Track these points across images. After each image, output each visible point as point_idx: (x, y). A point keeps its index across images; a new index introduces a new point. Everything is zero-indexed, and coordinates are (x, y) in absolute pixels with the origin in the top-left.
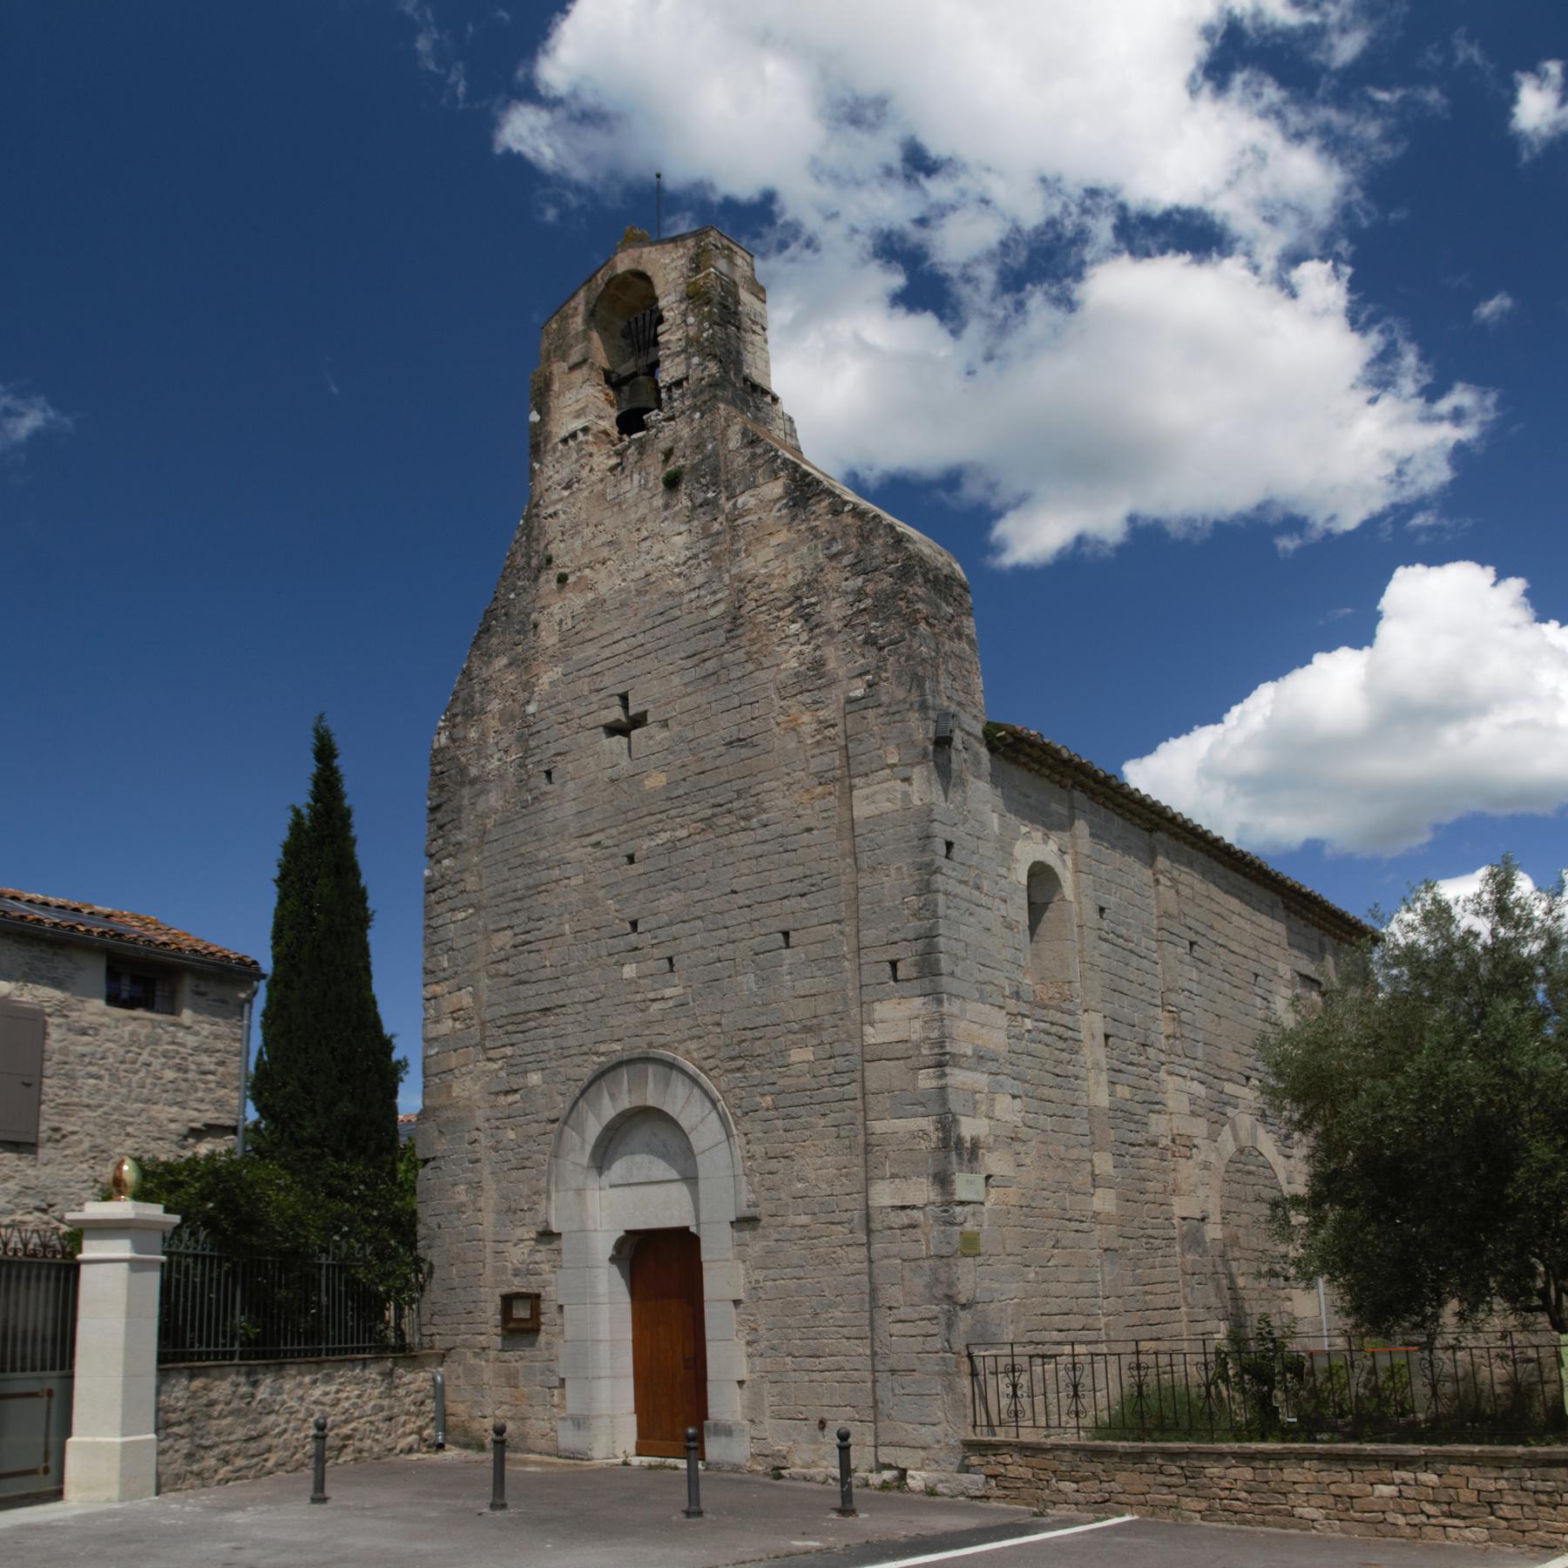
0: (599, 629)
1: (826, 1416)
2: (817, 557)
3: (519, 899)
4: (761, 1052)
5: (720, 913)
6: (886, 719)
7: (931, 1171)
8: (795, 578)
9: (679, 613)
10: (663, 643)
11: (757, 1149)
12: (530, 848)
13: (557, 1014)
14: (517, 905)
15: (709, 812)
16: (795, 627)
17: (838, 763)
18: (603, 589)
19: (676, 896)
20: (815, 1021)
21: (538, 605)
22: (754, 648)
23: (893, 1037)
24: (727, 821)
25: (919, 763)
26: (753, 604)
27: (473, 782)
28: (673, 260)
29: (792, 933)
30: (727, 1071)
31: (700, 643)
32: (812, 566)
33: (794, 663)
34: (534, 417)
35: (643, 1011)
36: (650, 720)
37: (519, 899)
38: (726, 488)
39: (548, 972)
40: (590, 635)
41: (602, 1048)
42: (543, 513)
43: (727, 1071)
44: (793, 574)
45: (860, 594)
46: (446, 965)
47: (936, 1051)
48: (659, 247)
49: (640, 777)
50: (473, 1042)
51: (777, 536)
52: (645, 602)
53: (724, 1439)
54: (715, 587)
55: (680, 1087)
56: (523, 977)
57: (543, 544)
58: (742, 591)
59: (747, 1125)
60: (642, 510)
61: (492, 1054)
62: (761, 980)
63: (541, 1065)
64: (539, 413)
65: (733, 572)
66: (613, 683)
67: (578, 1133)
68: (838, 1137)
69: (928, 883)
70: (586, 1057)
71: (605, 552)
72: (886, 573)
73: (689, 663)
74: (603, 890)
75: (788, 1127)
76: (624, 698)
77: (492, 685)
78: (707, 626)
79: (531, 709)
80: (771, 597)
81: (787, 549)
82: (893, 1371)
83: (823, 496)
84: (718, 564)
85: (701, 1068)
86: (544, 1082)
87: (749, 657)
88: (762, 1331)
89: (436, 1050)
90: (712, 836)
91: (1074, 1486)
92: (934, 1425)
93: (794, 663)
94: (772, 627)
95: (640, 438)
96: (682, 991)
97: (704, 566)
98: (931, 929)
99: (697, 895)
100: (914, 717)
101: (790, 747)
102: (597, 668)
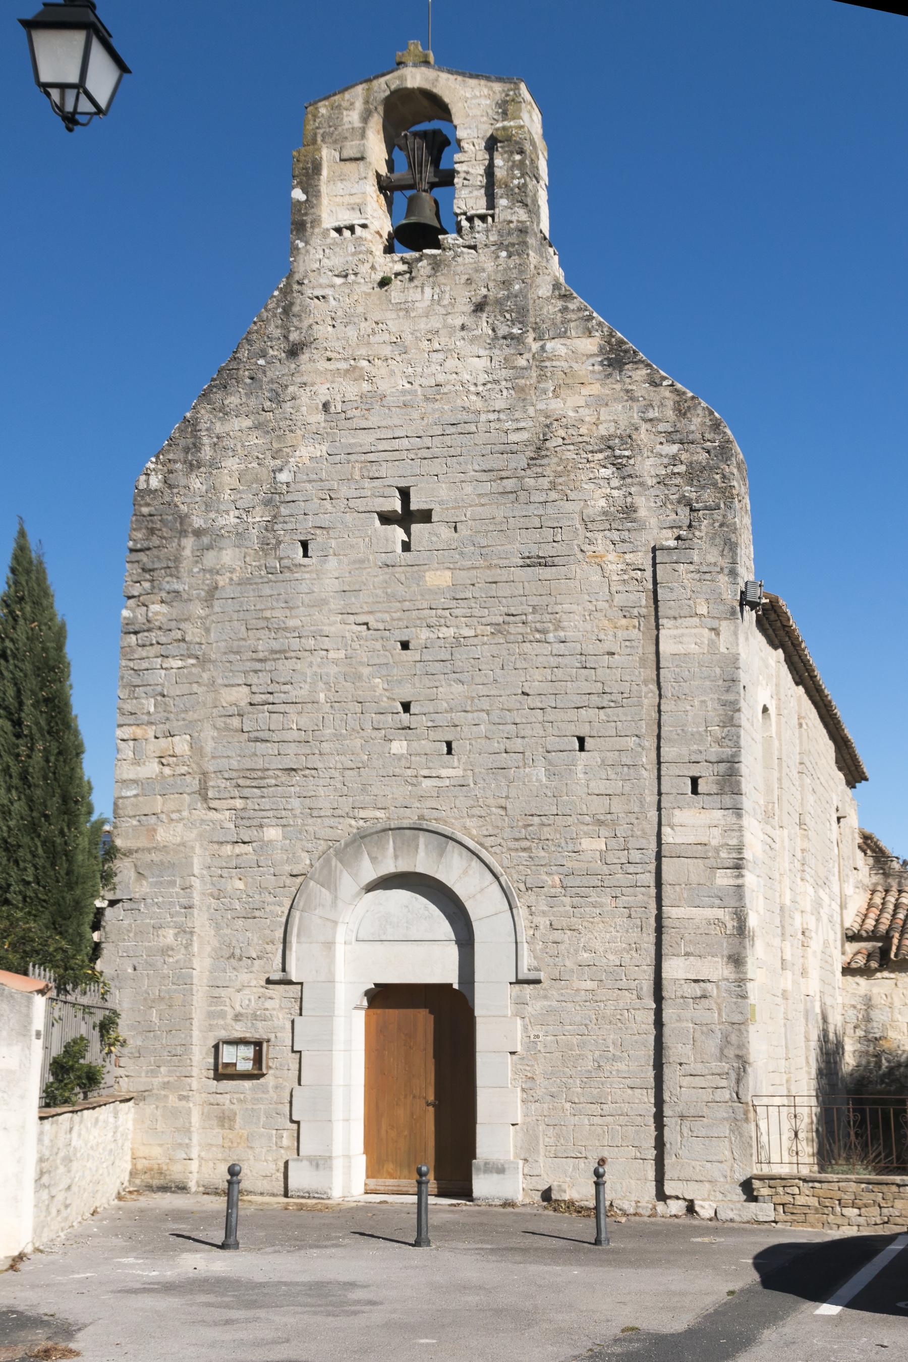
0: (373, 420)
1: (606, 1154)
2: (632, 417)
3: (260, 660)
4: (549, 837)
5: (508, 710)
6: (697, 576)
7: (726, 953)
8: (607, 429)
9: (474, 429)
10: (452, 451)
11: (543, 922)
12: (276, 613)
13: (305, 776)
14: (258, 666)
15: (501, 620)
16: (604, 472)
17: (644, 602)
18: (384, 386)
19: (458, 688)
20: (609, 816)
21: (298, 380)
22: (560, 480)
23: (692, 840)
24: (520, 630)
25: (726, 619)
26: (560, 441)
27: (198, 533)
28: (475, 97)
29: (587, 740)
30: (510, 849)
31: (496, 462)
32: (626, 423)
33: (602, 503)
34: (298, 194)
35: (412, 784)
36: (434, 519)
37: (260, 660)
38: (534, 329)
39: (295, 735)
40: (364, 424)
41: (362, 814)
42: (308, 292)
43: (510, 849)
44: (605, 425)
45: (675, 459)
46: (152, 710)
47: (735, 855)
48: (460, 78)
49: (422, 568)
50: (188, 790)
51: (589, 387)
52: (434, 410)
53: (495, 1177)
54: (518, 415)
55: (456, 858)
56: (261, 735)
57: (305, 324)
58: (547, 426)
59: (531, 898)
60: (435, 323)
61: (214, 804)
62: (550, 775)
63: (284, 821)
64: (305, 192)
65: (538, 407)
66: (394, 474)
67: (329, 889)
68: (630, 917)
69: (732, 718)
70: (341, 820)
71: (387, 351)
72: (703, 448)
73: (484, 477)
74: (370, 668)
75: (575, 904)
76: (405, 494)
77: (226, 442)
78: (508, 448)
79: (283, 477)
80: (580, 439)
81: (600, 402)
82: (682, 1117)
83: (641, 366)
84: (523, 396)
85: (481, 845)
86: (285, 838)
87: (553, 486)
88: (539, 1080)
89: (134, 792)
90: (502, 641)
91: (856, 1211)
92: (721, 1162)
93: (602, 503)
94: (580, 466)
95: (435, 256)
96: (461, 773)
97: (505, 392)
98: (732, 756)
99: (483, 690)
100: (723, 579)
101: (594, 579)
102: (371, 457)
